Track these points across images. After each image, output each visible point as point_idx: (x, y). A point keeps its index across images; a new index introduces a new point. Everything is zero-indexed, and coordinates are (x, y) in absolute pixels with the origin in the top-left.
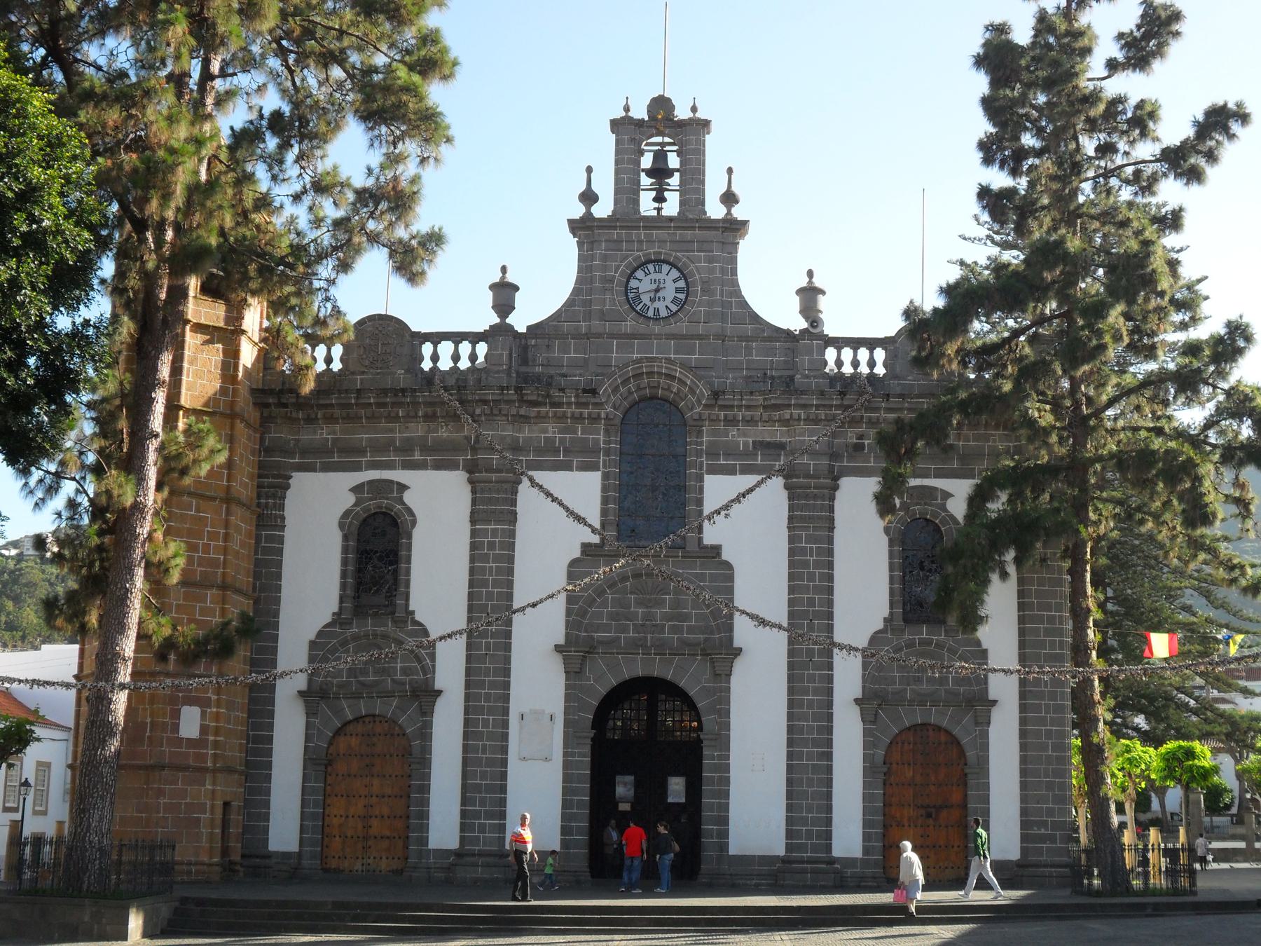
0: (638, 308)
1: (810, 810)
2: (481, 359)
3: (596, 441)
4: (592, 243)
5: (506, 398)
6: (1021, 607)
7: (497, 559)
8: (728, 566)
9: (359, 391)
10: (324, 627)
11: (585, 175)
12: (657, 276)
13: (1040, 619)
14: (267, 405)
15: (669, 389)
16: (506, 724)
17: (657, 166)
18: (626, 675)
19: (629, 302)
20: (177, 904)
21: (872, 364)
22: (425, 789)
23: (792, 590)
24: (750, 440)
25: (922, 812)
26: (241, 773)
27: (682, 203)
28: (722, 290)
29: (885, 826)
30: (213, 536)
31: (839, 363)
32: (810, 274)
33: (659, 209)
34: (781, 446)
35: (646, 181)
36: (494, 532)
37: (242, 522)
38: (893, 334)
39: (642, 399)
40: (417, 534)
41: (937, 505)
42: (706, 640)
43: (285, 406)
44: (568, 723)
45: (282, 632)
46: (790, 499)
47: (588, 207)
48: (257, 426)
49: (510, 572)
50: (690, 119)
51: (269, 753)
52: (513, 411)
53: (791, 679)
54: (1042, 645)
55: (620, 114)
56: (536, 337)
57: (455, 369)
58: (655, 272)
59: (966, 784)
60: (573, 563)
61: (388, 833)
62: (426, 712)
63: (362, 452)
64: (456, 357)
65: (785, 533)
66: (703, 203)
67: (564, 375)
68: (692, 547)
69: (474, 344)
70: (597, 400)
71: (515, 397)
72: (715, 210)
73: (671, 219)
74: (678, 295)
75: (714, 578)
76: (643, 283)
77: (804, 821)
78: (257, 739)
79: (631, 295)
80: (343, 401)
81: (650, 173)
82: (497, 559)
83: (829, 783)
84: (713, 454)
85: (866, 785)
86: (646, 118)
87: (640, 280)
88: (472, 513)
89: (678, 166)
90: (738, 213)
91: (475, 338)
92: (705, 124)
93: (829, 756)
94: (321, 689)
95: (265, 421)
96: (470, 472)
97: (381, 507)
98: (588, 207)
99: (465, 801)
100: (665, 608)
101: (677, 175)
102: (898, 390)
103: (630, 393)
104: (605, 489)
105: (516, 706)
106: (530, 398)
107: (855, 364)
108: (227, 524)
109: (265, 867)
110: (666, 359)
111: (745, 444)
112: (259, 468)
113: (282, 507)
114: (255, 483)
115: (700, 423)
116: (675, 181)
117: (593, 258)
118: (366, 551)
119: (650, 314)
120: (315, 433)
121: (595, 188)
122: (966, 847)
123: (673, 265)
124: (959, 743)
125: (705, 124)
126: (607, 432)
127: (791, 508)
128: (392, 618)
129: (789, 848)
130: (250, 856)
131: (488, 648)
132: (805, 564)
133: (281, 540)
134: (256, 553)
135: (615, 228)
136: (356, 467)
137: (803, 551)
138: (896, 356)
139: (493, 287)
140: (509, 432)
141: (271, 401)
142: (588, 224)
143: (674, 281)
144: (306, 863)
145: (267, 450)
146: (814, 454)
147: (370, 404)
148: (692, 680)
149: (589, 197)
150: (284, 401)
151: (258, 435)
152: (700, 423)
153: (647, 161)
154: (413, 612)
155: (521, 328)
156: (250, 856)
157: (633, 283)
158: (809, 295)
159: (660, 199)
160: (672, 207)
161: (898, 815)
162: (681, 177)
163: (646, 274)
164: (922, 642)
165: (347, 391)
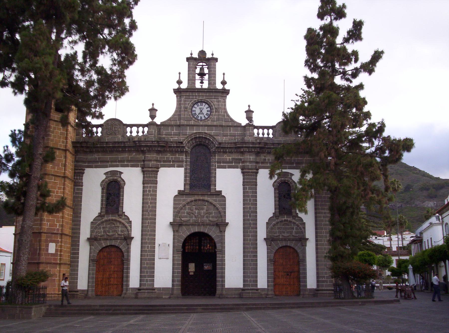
0: (195, 117)
1: (250, 273)
2: (146, 133)
3: (182, 158)
4: (181, 96)
6: (316, 209)
7: (151, 195)
8: (224, 197)
9: (107, 142)
10: (96, 217)
11: (179, 75)
13: (322, 213)
14: (77, 147)
16: (154, 247)
18: (193, 231)
19: (192, 115)
20: (48, 307)
21: (268, 134)
22: (128, 268)
23: (244, 204)
24: (231, 158)
26: (68, 264)
29: (274, 279)
30: (59, 188)
31: (258, 134)
32: (249, 106)
33: (202, 86)
34: (241, 159)
35: (197, 77)
36: (150, 187)
37: (69, 185)
38: (275, 125)
39: (197, 145)
40: (126, 188)
41: (289, 178)
42: (217, 220)
44: (174, 247)
45: (82, 219)
46: (243, 176)
48: (74, 153)
49: (156, 199)
50: (211, 58)
51: (78, 258)
52: (156, 149)
53: (244, 232)
54: (322, 221)
55: (189, 56)
57: (137, 135)
58: (201, 105)
59: (299, 265)
61: (116, 283)
62: (129, 244)
63: (108, 162)
64: (138, 132)
65: (242, 187)
66: (215, 84)
68: (212, 191)
70: (183, 145)
72: (219, 86)
73: (205, 89)
74: (208, 113)
75: (220, 201)
76: (197, 109)
77: (249, 277)
78: (74, 254)
80: (101, 146)
81: (199, 74)
82: (151, 195)
86: (198, 57)
87: (196, 108)
88: (143, 181)
89: (207, 72)
90: (227, 87)
91: (144, 126)
92: (216, 60)
93: (256, 256)
94: (95, 237)
96: (143, 168)
97: (114, 179)
101: (207, 75)
102: (276, 142)
103: (193, 143)
104: (185, 173)
105: (157, 242)
107: (263, 134)
108: (64, 184)
109: (76, 295)
110: (204, 132)
111: (229, 159)
113: (82, 179)
114: (73, 172)
116: (206, 77)
117: (181, 101)
118: (109, 193)
119: (199, 118)
120: (93, 156)
121: (181, 79)
122: (300, 284)
123: (206, 103)
125: (216, 60)
126: (186, 156)
127: (244, 179)
128: (118, 214)
129: (244, 285)
130: (72, 291)
132: (248, 196)
133: (82, 190)
134: (74, 194)
135: (188, 91)
137: (248, 192)
138: (276, 131)
139: (150, 110)
141: (78, 145)
142: (179, 90)
143: (207, 108)
144: (90, 293)
145: (76, 161)
146: (251, 162)
148: (213, 232)
149: (179, 82)
150: (82, 145)
151: (74, 156)
153: (198, 71)
154: (124, 212)
155: (159, 123)
156: (72, 291)
157: (194, 109)
158: (249, 113)
159: (202, 82)
160: (206, 85)
162: (209, 75)
163: (198, 106)
164: (285, 221)
165: (103, 142)
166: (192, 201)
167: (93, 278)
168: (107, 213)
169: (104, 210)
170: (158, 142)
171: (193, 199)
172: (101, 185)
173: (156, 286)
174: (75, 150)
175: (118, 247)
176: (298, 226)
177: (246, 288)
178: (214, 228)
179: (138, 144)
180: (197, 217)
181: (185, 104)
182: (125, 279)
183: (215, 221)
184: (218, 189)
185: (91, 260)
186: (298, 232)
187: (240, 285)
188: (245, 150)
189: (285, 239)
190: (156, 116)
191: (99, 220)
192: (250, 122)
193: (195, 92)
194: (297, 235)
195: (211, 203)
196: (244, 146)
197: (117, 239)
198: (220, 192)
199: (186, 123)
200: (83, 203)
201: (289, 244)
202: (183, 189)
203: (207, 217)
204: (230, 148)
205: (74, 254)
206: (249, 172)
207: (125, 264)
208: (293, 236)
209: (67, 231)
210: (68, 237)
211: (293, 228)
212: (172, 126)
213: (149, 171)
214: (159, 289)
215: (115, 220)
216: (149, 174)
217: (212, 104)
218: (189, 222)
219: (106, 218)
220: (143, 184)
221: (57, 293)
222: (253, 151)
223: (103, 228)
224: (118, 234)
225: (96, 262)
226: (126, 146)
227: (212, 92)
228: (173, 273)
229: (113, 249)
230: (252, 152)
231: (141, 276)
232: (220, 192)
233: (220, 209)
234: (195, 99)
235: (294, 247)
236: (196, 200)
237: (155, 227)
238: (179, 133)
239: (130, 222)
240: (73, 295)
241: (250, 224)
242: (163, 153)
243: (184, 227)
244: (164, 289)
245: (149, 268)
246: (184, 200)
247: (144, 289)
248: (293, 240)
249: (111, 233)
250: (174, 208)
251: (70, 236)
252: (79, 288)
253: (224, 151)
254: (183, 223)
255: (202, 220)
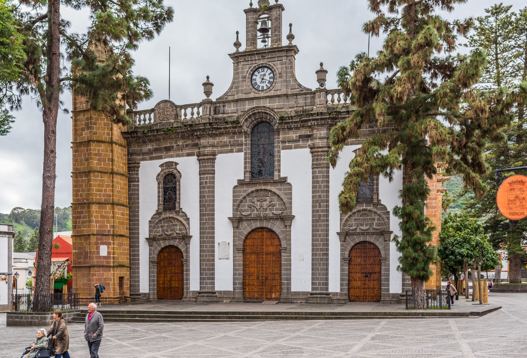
0: (256, 87)
1: (319, 275)
3: (242, 141)
4: (238, 63)
5: (206, 127)
7: (208, 187)
8: (289, 184)
10: (153, 215)
11: (236, 35)
12: (263, 73)
14: (129, 138)
15: (266, 118)
16: (213, 247)
17: (262, 27)
25: (364, 275)
26: (127, 267)
27: (272, 42)
28: (286, 76)
31: (333, 101)
32: (321, 64)
35: (259, 34)
37: (121, 183)
39: (259, 123)
40: (182, 180)
42: (282, 213)
43: (134, 137)
44: (234, 245)
47: (237, 48)
48: (126, 145)
49: (213, 192)
51: (138, 260)
52: (210, 132)
55: (248, 7)
56: (219, 103)
58: (262, 71)
60: (235, 187)
62: (187, 244)
64: (192, 114)
65: (311, 170)
67: (229, 117)
68: (276, 178)
69: (198, 108)
71: (209, 127)
72: (285, 42)
75: (285, 189)
76: (257, 78)
77: (318, 279)
78: (134, 255)
79: (253, 82)
80: (153, 134)
82: (208, 187)
83: (327, 265)
84: (283, 142)
85: (342, 265)
86: (258, 7)
87: (256, 76)
90: (294, 43)
91: (199, 105)
93: (327, 255)
94: (154, 237)
95: (129, 145)
96: (198, 156)
97: (169, 172)
98: (237, 48)
99: (201, 274)
100: (267, 202)
104: (245, 158)
105: (217, 240)
106: (215, 126)
112: (128, 161)
113: (138, 174)
114: (127, 166)
115: (279, 130)
117: (238, 69)
118: (166, 188)
119: (260, 89)
120: (147, 146)
124: (378, 248)
126: (246, 137)
129: (313, 289)
131: (206, 220)
132: (318, 182)
133: (138, 186)
134: (129, 191)
135: (245, 55)
136: (160, 158)
137: (317, 177)
139: (204, 84)
140: (211, 141)
143: (269, 74)
144: (151, 297)
145: (129, 154)
146: (321, 138)
147: (162, 134)
148: (277, 227)
149: (237, 44)
150: (133, 136)
151: (126, 149)
152: (279, 130)
153: (259, 26)
154: (181, 209)
155: (214, 100)
157: (254, 77)
160: (269, 43)
161: (355, 276)
163: (259, 73)
164: (363, 210)
166: (252, 192)
167: (153, 281)
168: (165, 210)
169: (161, 207)
170: (210, 124)
171: (254, 189)
172: (157, 179)
173: (217, 289)
174: (127, 142)
175: (177, 248)
176: (379, 215)
177: (314, 292)
178: (278, 223)
179: (189, 129)
180: (259, 210)
181: (243, 72)
182: (185, 282)
183: (279, 214)
184: (282, 175)
185: (151, 262)
186: (380, 224)
187: (308, 288)
188: (313, 124)
189: (363, 233)
190: (212, 93)
191: (156, 218)
192: (322, 87)
193: (254, 54)
194: (379, 228)
195: (275, 193)
196: (311, 118)
197: (175, 238)
198: (285, 178)
199: (244, 96)
200: (141, 201)
201: (368, 239)
202: (243, 178)
203: (270, 210)
204: (296, 122)
205: (134, 255)
206: (319, 152)
207: (185, 265)
208: (373, 229)
209: (125, 231)
210: (124, 238)
211: (374, 219)
212: (229, 102)
213: (204, 159)
214: (220, 292)
215: (173, 218)
216: (205, 162)
217: (275, 68)
218: (250, 217)
219: (163, 216)
220: (200, 175)
221: (113, 297)
222: (323, 125)
223: (162, 227)
224: (176, 233)
225: (157, 263)
226: (179, 132)
227: (275, 52)
228: (234, 274)
229: (173, 250)
230: (322, 125)
231: (201, 279)
232: (285, 178)
233: (285, 200)
234: (255, 64)
235: (374, 242)
236: (257, 191)
237: (213, 224)
238: (237, 110)
239: (188, 219)
240: (134, 298)
241: (320, 216)
242: (220, 136)
243: (245, 224)
244: (225, 292)
245: (209, 269)
246: (244, 191)
247: (203, 293)
248: (373, 234)
249: (169, 233)
250: (234, 201)
251: (127, 237)
252: (141, 291)
253: (289, 127)
254: (242, 218)
255: (265, 214)
